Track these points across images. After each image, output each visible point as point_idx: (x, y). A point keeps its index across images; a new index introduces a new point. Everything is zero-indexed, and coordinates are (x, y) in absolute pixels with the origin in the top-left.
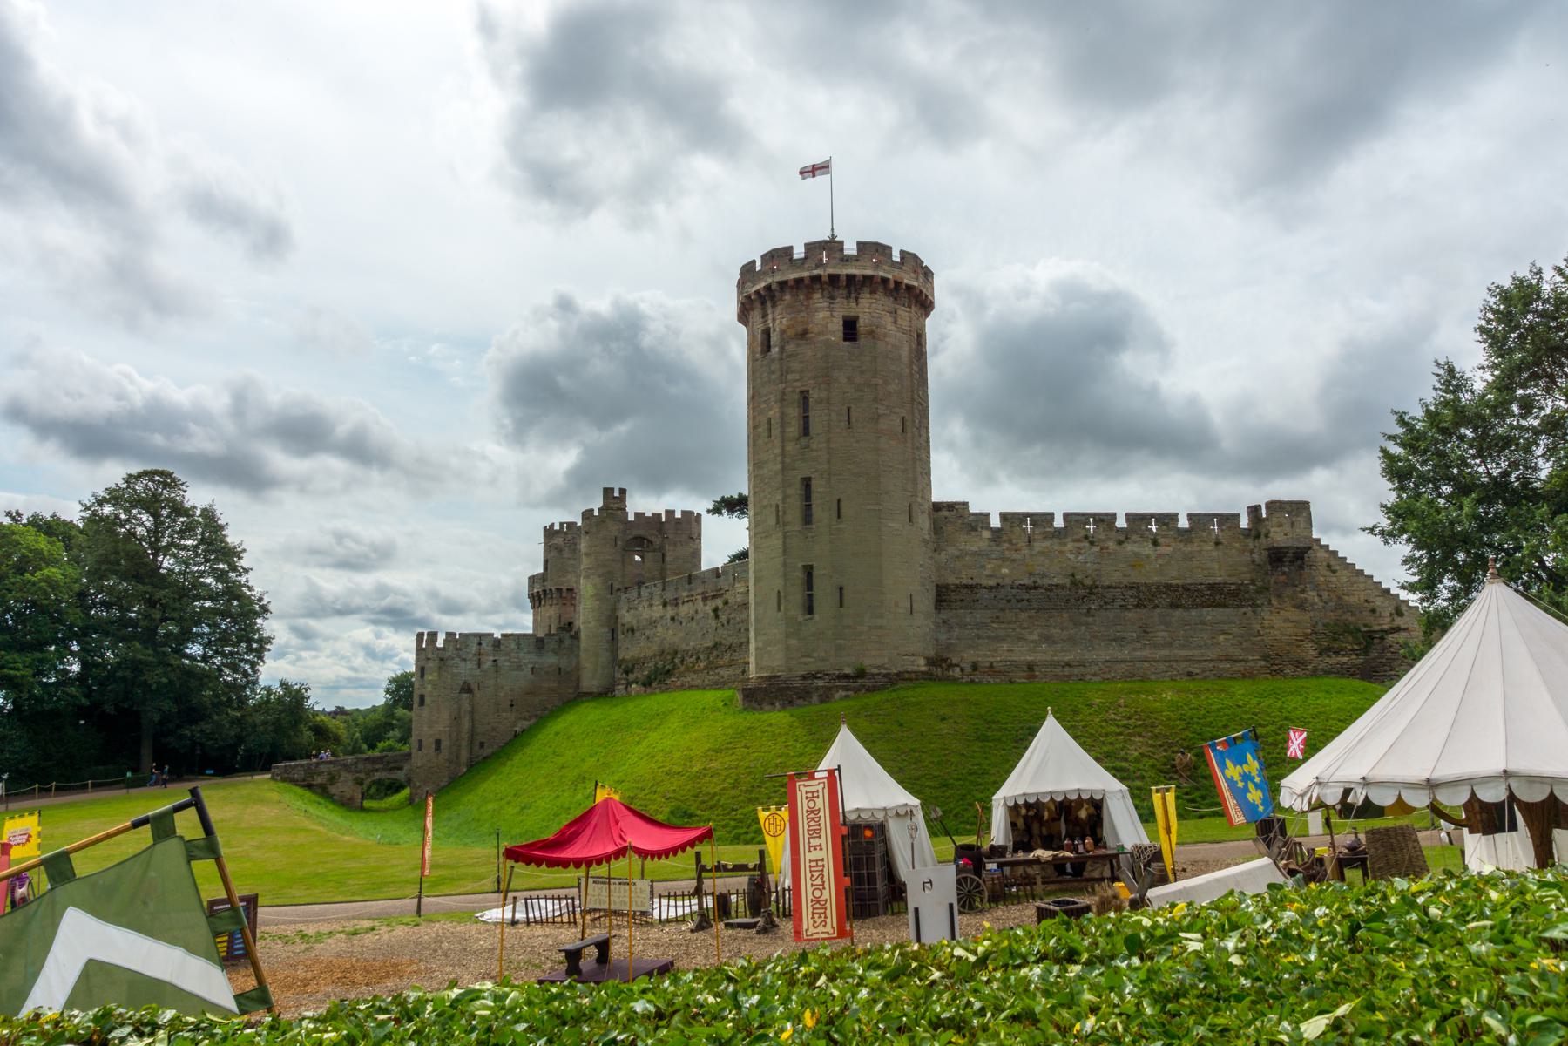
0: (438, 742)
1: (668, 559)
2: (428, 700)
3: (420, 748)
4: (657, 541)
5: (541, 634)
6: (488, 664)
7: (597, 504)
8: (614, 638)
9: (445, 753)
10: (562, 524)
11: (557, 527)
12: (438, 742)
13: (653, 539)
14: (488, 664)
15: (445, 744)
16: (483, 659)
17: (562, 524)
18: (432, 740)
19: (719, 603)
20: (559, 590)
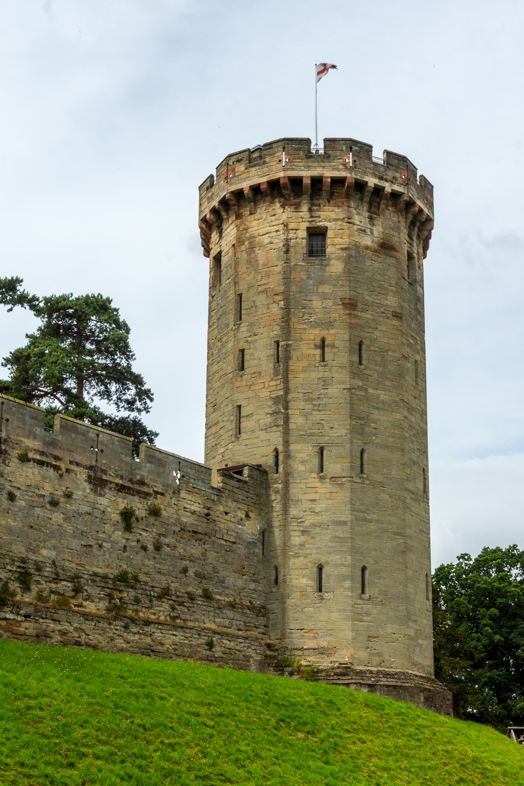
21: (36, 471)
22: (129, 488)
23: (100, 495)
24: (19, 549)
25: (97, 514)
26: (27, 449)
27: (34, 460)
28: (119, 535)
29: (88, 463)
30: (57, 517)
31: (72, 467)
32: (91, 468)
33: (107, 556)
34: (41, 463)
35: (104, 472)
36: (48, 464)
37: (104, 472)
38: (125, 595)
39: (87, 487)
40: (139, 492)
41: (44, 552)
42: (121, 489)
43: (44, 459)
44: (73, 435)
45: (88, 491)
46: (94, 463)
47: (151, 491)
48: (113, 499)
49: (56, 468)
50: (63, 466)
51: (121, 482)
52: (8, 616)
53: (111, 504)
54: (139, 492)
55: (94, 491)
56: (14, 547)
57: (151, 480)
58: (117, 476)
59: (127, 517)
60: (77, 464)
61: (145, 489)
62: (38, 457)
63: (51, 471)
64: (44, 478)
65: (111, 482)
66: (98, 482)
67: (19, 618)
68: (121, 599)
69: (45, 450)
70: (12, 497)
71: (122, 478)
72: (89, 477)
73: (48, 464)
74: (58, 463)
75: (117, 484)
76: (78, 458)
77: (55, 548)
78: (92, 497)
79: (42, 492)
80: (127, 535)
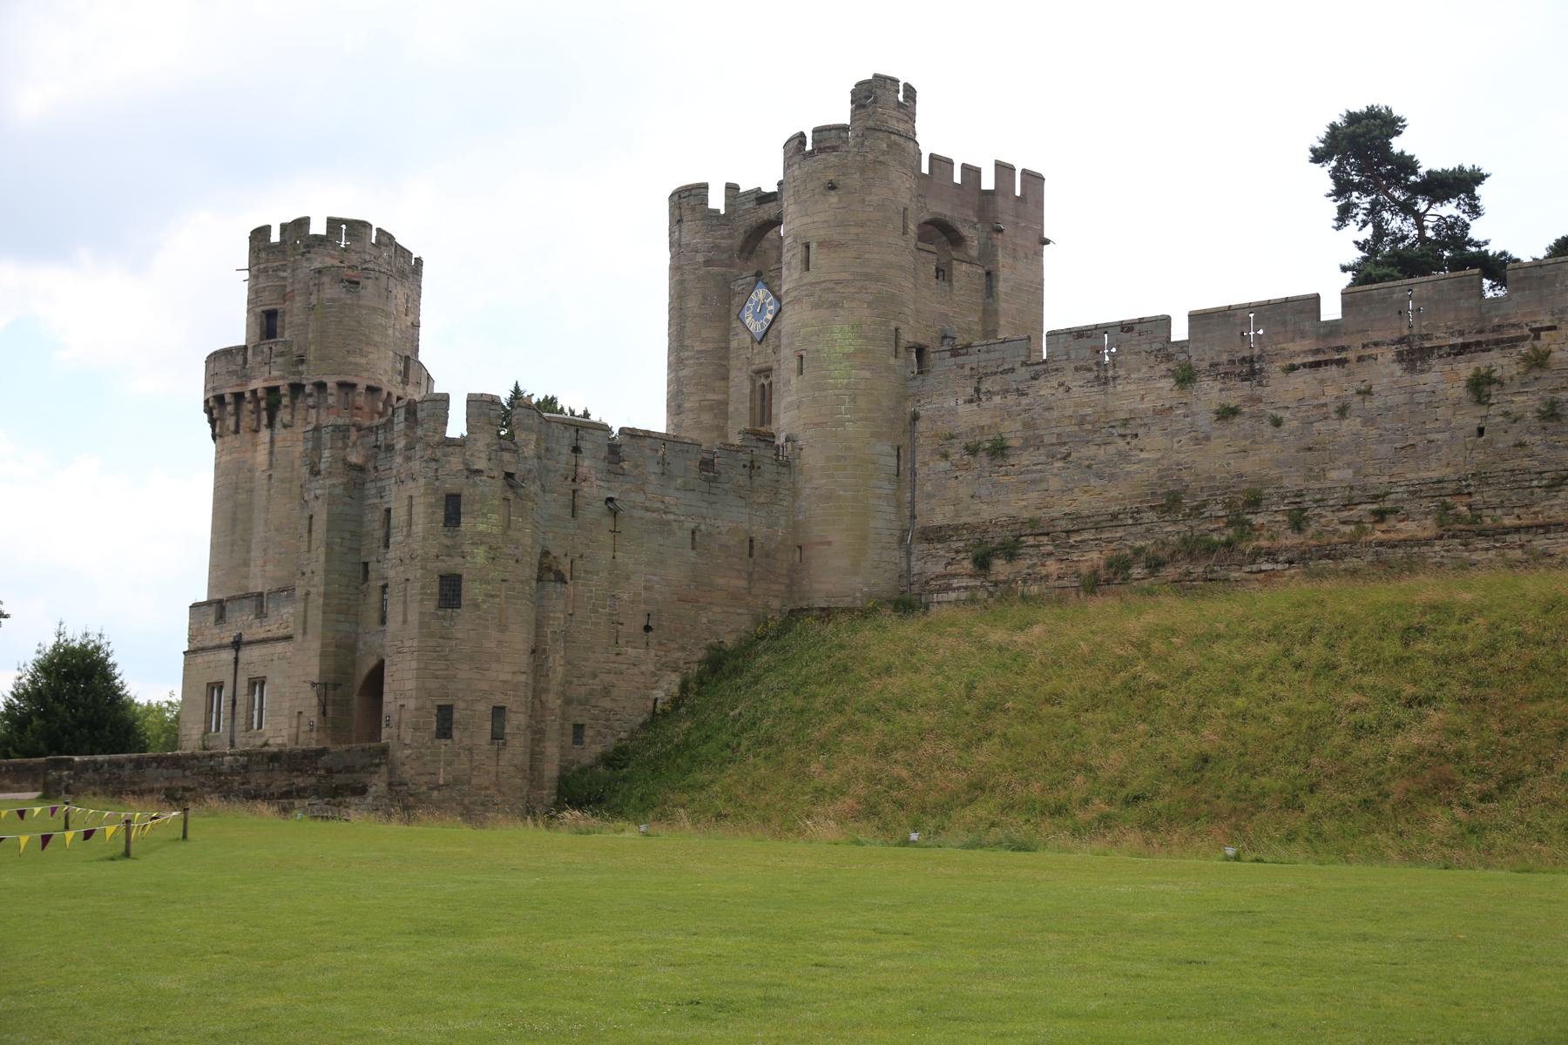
0: (499, 712)
1: (1002, 287)
2: (471, 590)
3: (444, 731)
4: (973, 237)
5: (708, 440)
6: (594, 511)
7: (840, 113)
8: (904, 474)
9: (517, 747)
10: (333, 223)
11: (318, 228)
12: (499, 712)
13: (965, 231)
14: (594, 511)
15: (517, 720)
16: (586, 489)
17: (333, 223)
18: (484, 708)
19: (1502, 363)
20: (347, 387)
21: (1309, 378)
22: (1478, 343)
23: (1422, 371)
24: (1293, 482)
25: (1422, 398)
26: (1294, 355)
27: (1304, 365)
28: (1470, 418)
29: (1396, 336)
30: (1352, 424)
31: (1368, 352)
32: (1401, 341)
33: (1445, 450)
34: (1317, 365)
35: (1428, 337)
36: (1326, 363)
37: (1428, 337)
38: (1477, 497)
39: (1397, 369)
40: (1498, 343)
41: (1333, 475)
42: (1463, 349)
43: (1320, 357)
44: (1365, 309)
45: (1399, 373)
46: (1406, 332)
47: (1526, 331)
48: (1448, 368)
49: (1341, 363)
50: (1351, 355)
51: (1460, 340)
52: (1263, 567)
53: (1446, 380)
54: (1498, 343)
55: (1411, 369)
56: (1286, 482)
57: (1524, 315)
58: (1452, 334)
59: (1480, 386)
60: (1376, 344)
61: (1513, 333)
62: (1311, 359)
63: (1334, 370)
64: (1322, 382)
65: (1440, 348)
66: (1413, 355)
67: (1279, 567)
68: (1470, 507)
69: (1321, 345)
70: (1277, 423)
71: (1461, 333)
72: (1399, 354)
73: (1326, 363)
74: (1343, 355)
75: (1451, 346)
76: (1376, 336)
77: (1349, 465)
78: (1408, 379)
79: (1323, 400)
80: (1482, 411)
